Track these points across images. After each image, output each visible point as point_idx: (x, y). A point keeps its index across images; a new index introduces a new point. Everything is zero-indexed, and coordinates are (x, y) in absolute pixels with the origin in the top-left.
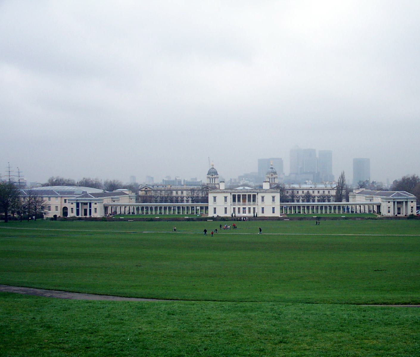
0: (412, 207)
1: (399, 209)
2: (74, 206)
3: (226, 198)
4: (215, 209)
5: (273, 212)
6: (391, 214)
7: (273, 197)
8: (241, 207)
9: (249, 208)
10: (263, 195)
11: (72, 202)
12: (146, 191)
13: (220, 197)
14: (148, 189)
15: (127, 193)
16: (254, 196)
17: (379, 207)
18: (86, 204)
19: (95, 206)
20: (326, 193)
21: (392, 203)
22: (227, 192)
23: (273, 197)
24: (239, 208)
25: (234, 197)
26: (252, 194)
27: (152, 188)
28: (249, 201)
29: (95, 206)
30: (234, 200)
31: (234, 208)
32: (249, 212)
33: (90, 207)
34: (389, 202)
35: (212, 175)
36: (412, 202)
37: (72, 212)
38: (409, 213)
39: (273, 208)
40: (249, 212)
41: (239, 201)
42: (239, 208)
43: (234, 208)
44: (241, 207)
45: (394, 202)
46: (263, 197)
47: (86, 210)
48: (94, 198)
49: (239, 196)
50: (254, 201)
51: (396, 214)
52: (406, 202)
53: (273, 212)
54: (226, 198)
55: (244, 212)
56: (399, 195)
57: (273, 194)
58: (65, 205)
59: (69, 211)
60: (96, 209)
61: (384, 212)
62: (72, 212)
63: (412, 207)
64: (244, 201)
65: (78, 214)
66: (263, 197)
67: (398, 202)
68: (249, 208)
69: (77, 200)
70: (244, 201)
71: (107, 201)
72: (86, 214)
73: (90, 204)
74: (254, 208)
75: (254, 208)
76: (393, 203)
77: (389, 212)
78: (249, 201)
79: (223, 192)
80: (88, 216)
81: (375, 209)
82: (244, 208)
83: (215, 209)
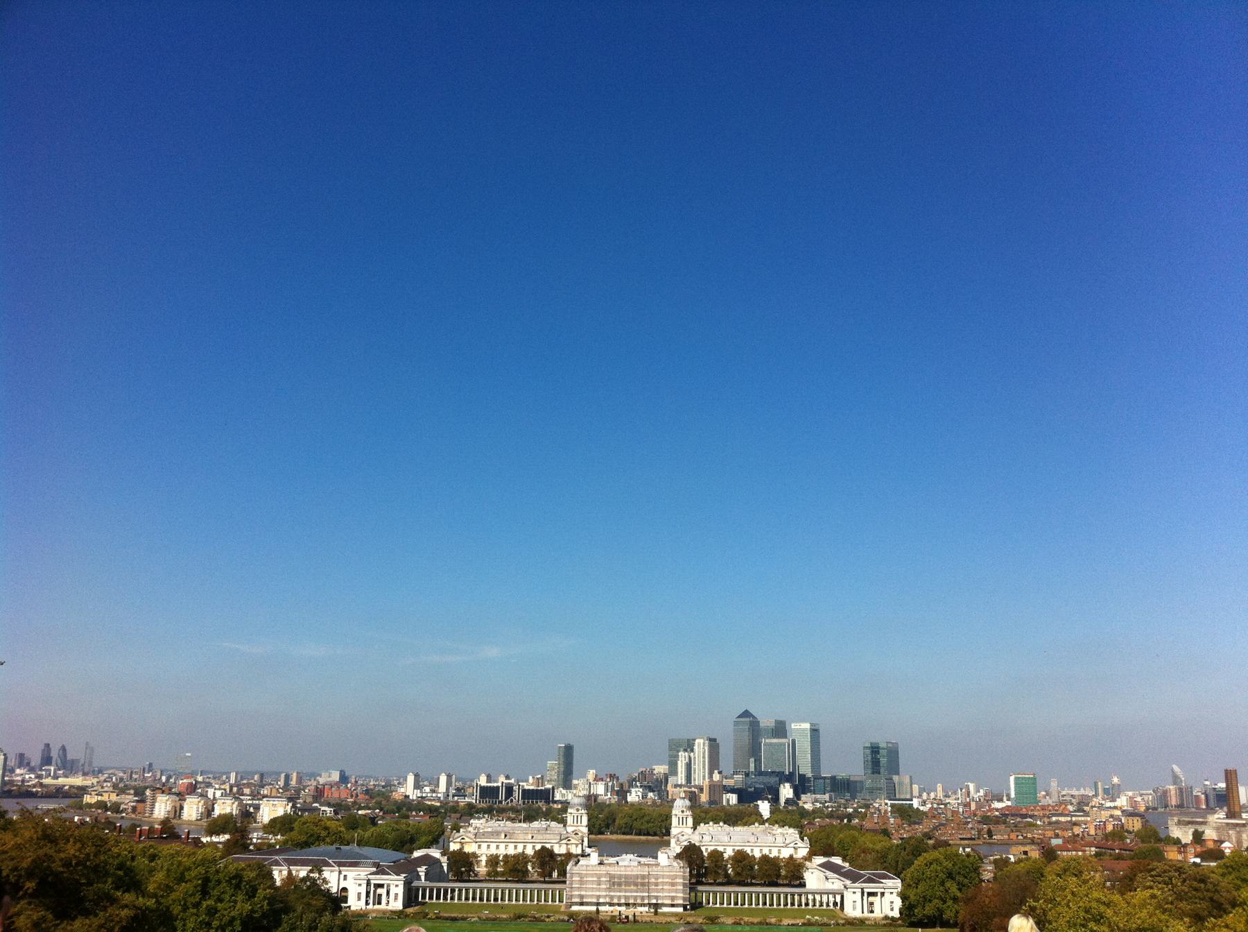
18: (381, 886)
20: (774, 854)
37: (359, 899)
52: (883, 894)
56: (870, 880)
62: (359, 899)
65: (367, 903)
67: (870, 894)
72: (379, 903)
73: (388, 885)
76: (859, 895)
81: (838, 899)
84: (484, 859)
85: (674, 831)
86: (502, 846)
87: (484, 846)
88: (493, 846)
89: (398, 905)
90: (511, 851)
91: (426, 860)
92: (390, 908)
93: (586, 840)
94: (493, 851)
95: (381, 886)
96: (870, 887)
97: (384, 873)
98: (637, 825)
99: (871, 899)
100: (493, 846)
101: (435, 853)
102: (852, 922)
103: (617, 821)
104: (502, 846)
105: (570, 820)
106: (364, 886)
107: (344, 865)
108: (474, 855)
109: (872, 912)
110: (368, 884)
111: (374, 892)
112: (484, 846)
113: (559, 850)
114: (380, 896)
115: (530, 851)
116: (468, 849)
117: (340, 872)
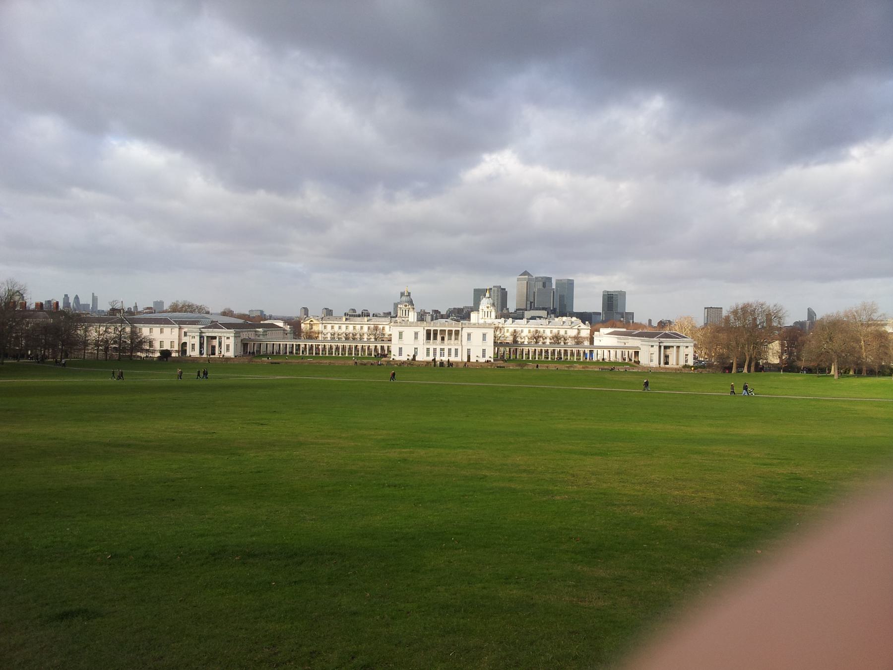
0: (687, 355)
1: (667, 357)
2: (196, 341)
3: (416, 334)
4: (400, 349)
5: (484, 356)
6: (655, 364)
8: (438, 348)
9: (450, 350)
11: (193, 334)
12: (311, 325)
13: (408, 332)
14: (315, 322)
16: (457, 332)
17: (637, 353)
18: (215, 338)
19: (228, 342)
21: (656, 348)
24: (435, 350)
25: (428, 333)
26: (454, 329)
29: (228, 342)
30: (428, 338)
31: (428, 349)
32: (449, 354)
34: (652, 346)
36: (687, 347)
38: (682, 363)
39: (484, 351)
40: (449, 354)
41: (435, 338)
42: (435, 350)
43: (428, 349)
44: (438, 348)
45: (660, 347)
46: (469, 335)
49: (435, 332)
51: (662, 364)
52: (678, 347)
53: (484, 356)
54: (416, 334)
55: (442, 355)
58: (184, 339)
59: (189, 348)
60: (228, 346)
61: (644, 360)
63: (687, 355)
64: (443, 339)
65: (201, 353)
66: (469, 335)
67: (666, 348)
68: (450, 350)
69: (201, 333)
70: (443, 339)
73: (220, 338)
74: (456, 350)
75: (456, 350)
77: (651, 361)
78: (450, 339)
79: (411, 325)
82: (442, 350)
83: (400, 349)
84: (329, 336)
86: (344, 327)
87: (329, 326)
88: (336, 327)
95: (215, 338)
96: (667, 342)
99: (668, 351)
100: (336, 327)
102: (649, 371)
104: (344, 327)
106: (197, 339)
107: (184, 323)
109: (667, 363)
110: (201, 337)
112: (329, 326)
114: (213, 347)
117: (180, 328)
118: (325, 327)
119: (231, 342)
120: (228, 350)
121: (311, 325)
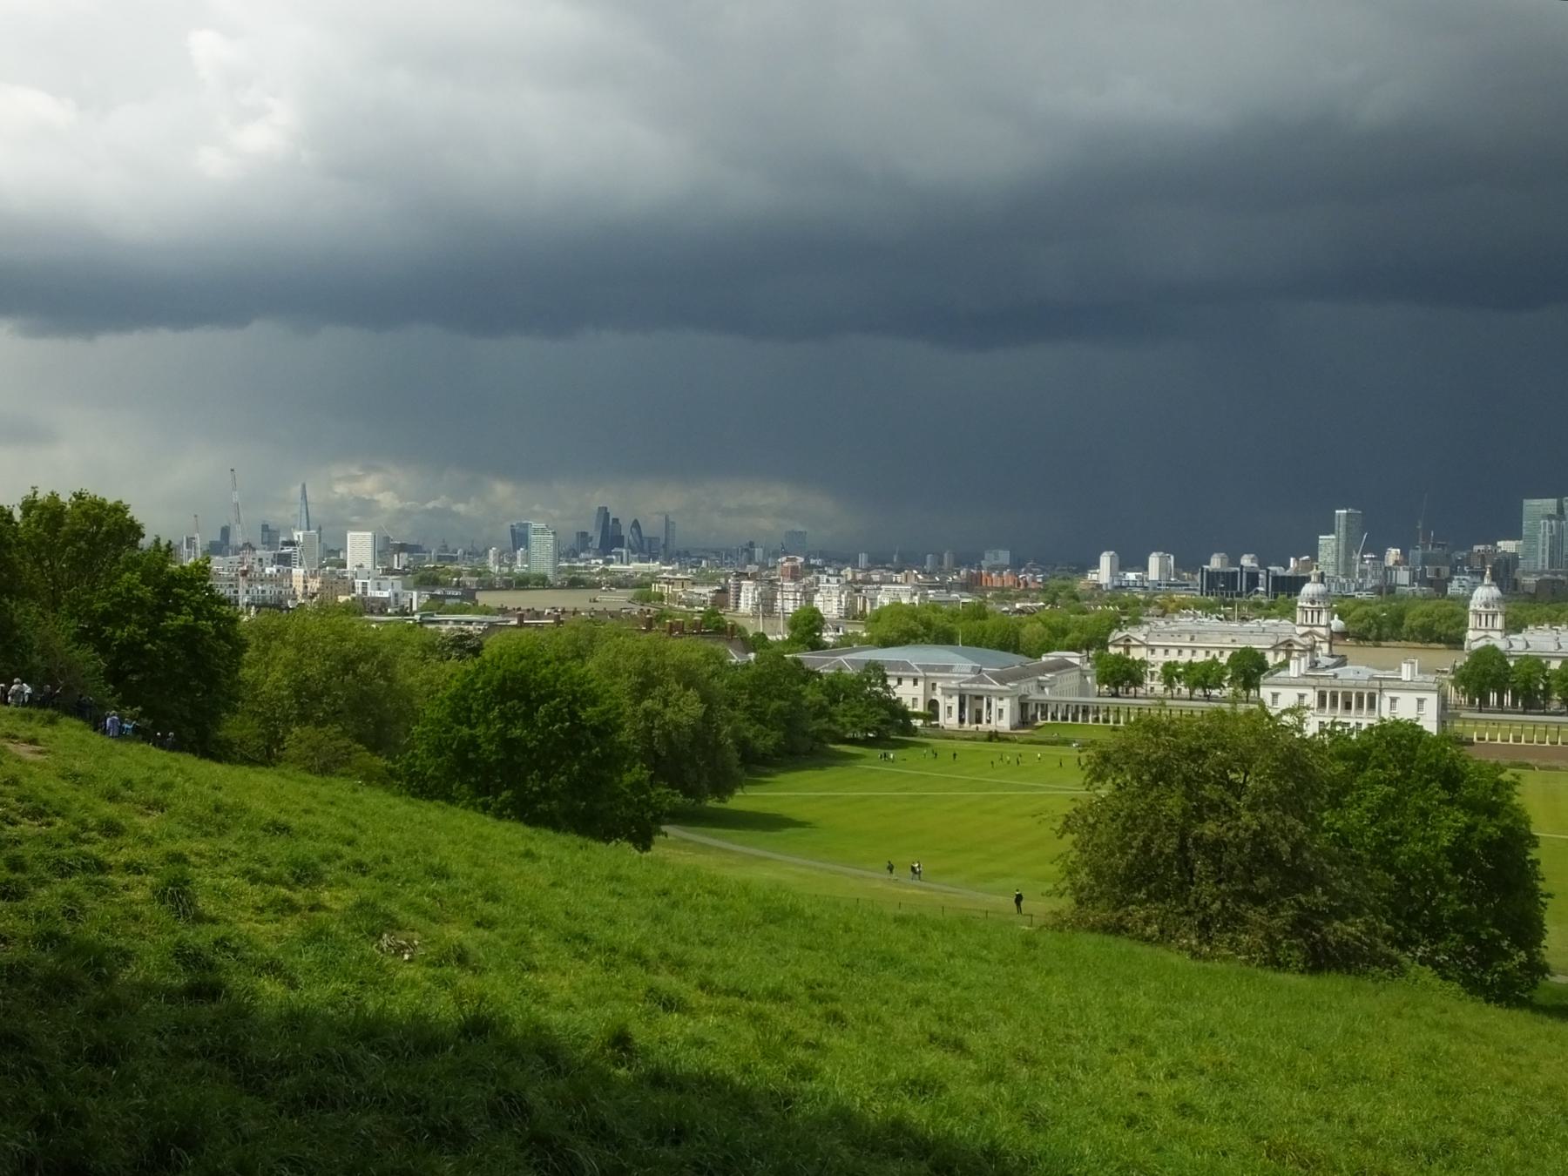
7: (1420, 701)
10: (1394, 694)
15: (1077, 661)
16: (1372, 698)
18: (980, 698)
22: (1305, 686)
23: (1420, 701)
25: (1322, 696)
27: (1142, 638)
28: (1360, 705)
29: (1000, 704)
30: (1322, 704)
33: (989, 705)
35: (1313, 602)
46: (1393, 700)
47: (979, 712)
48: (997, 686)
50: (1372, 706)
57: (1421, 695)
64: (1348, 706)
65: (962, 720)
66: (1393, 700)
70: (1348, 706)
71: (1028, 687)
72: (979, 721)
78: (1360, 705)
80: (983, 726)
84: (1158, 669)
85: (1470, 635)
86: (1187, 653)
87: (1160, 651)
89: (1004, 725)
90: (1200, 657)
91: (1065, 665)
92: (992, 727)
93: (1325, 646)
94: (1173, 656)
97: (982, 680)
98: (1441, 628)
100: (1173, 652)
101: (1074, 658)
103: (1407, 622)
105: (1299, 614)
106: (955, 701)
108: (1143, 663)
111: (971, 703)
112: (1160, 651)
113: (1271, 658)
115: (1223, 660)
116: (1137, 654)
118: (1153, 651)
119: (1006, 704)
120: (1000, 716)
121: (1127, 648)
